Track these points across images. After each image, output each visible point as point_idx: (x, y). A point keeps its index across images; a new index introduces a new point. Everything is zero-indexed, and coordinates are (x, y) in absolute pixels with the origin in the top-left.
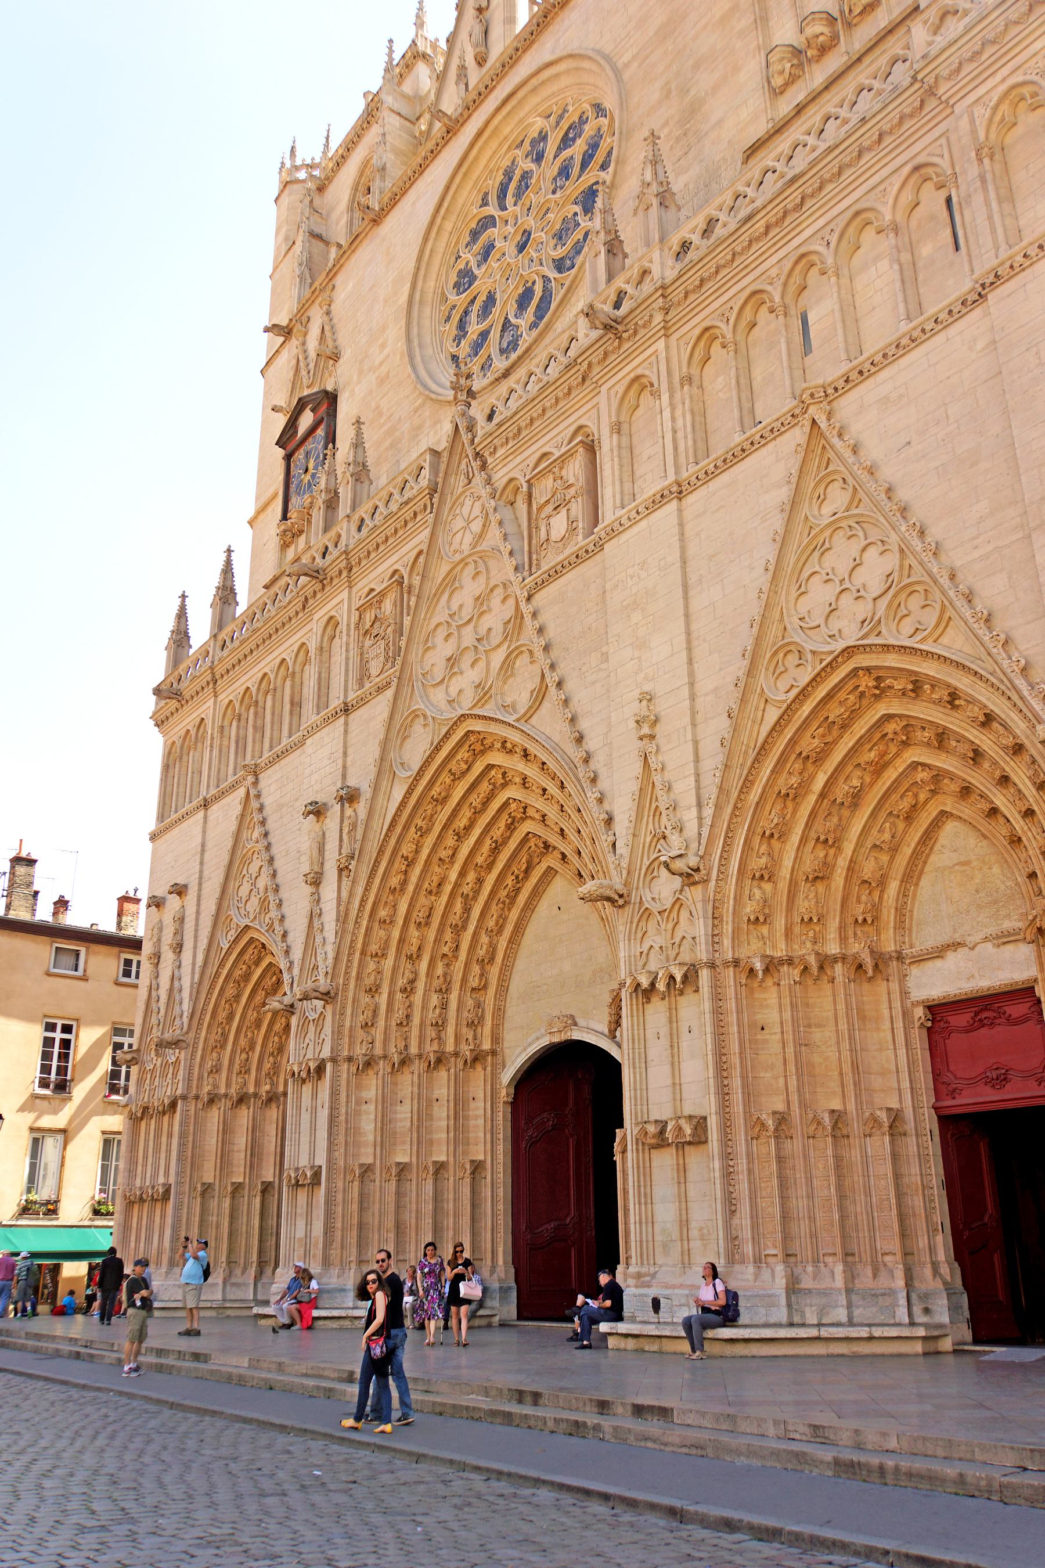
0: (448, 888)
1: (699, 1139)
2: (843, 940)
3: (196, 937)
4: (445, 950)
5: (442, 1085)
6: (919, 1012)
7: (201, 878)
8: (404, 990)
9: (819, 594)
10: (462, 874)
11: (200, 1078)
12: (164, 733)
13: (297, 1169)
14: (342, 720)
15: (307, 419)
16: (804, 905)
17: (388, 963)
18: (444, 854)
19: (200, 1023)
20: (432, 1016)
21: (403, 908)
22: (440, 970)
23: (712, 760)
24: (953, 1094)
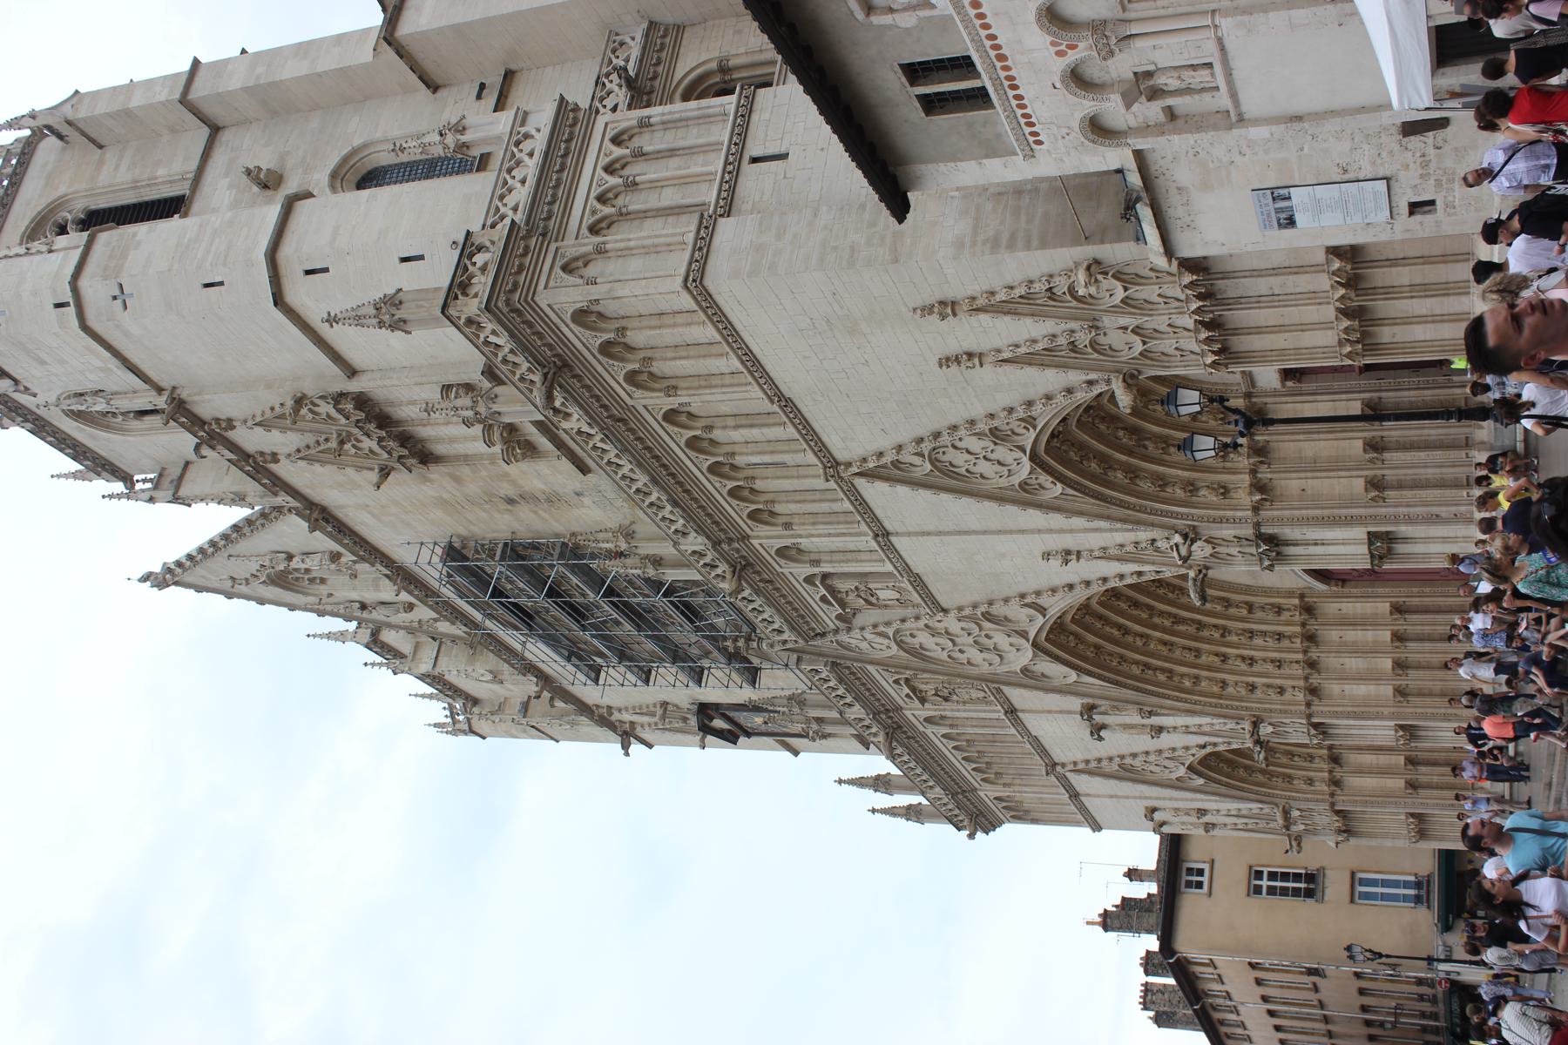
0: (1167, 637)
4: (1217, 635)
6: (1289, 384)
7: (1140, 798)
10: (1155, 627)
11: (1314, 792)
12: (1001, 823)
15: (719, 723)
18: (1139, 643)
19: (1269, 795)
20: (1271, 643)
22: (1234, 638)
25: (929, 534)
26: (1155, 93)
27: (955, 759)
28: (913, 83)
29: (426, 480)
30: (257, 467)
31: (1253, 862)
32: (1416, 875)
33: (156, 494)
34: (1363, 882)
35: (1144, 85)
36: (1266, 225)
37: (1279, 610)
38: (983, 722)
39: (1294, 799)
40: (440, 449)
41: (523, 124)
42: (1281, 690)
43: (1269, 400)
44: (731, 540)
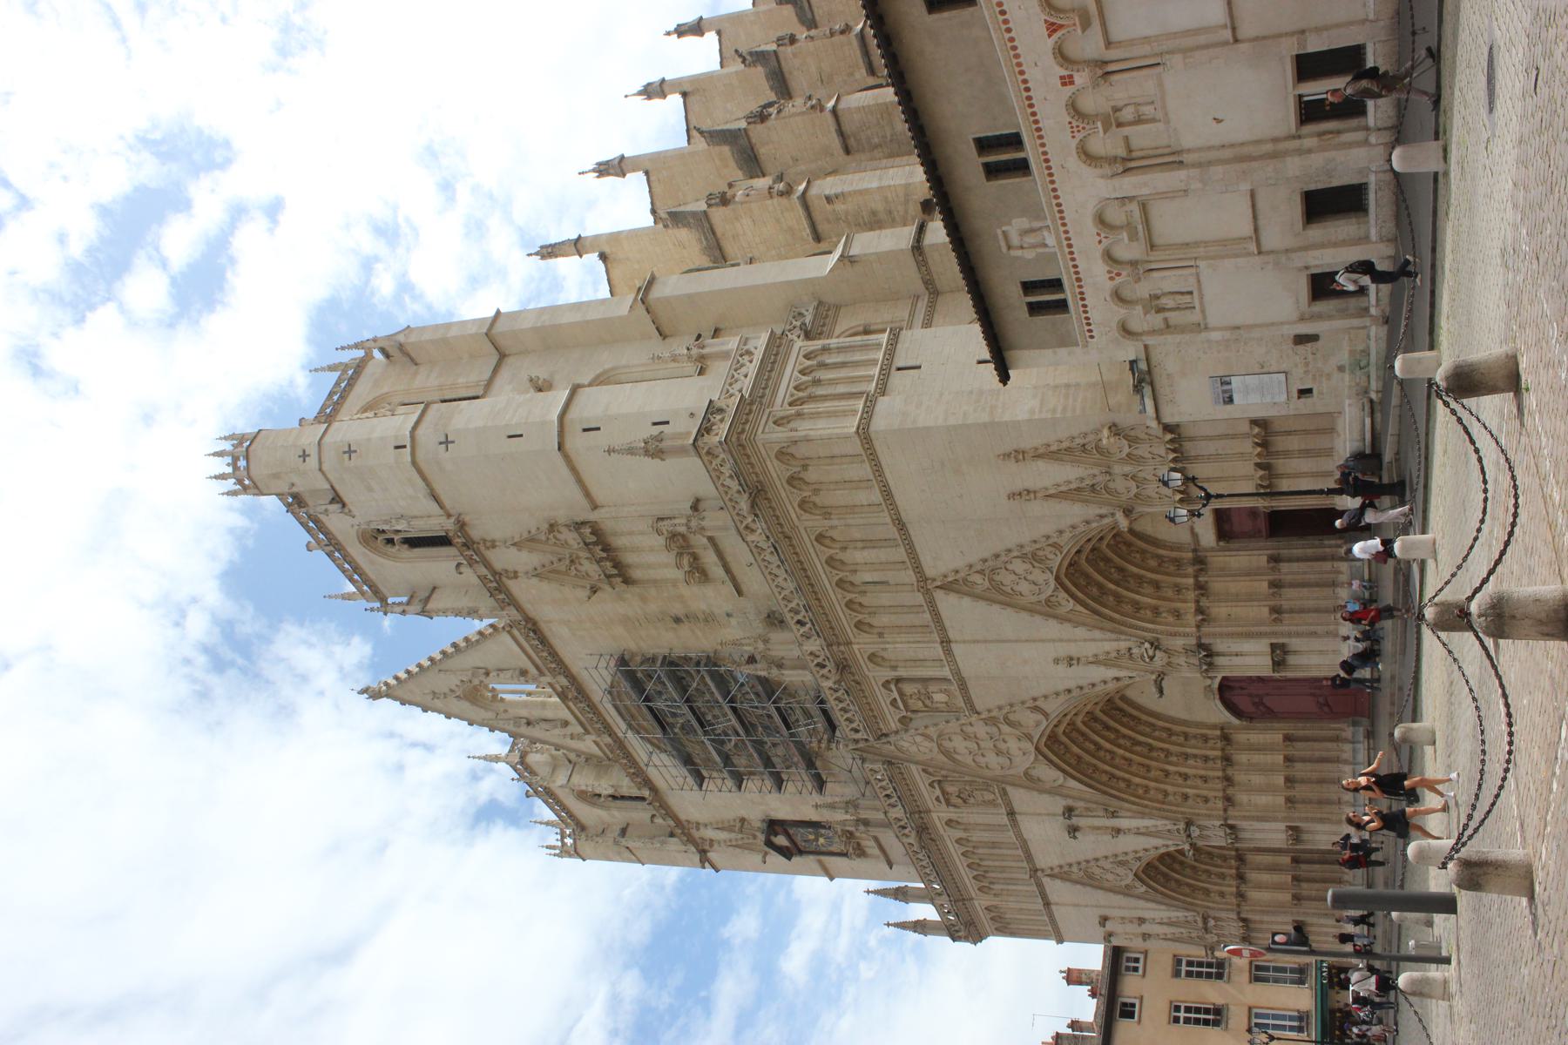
0: (1128, 755)
1: (1282, 647)
2: (1186, 576)
3: (1136, 908)
4: (1162, 756)
6: (1221, 544)
7: (1096, 906)
8: (1206, 781)
9: (1024, 587)
10: (1119, 746)
11: (1226, 903)
13: (1288, 840)
14: (1018, 817)
16: (1170, 593)
17: (1170, 788)
19: (1192, 904)
20: (1200, 763)
21: (1137, 780)
22: (1174, 759)
23: (1097, 634)
24: (1260, 531)
25: (978, 642)
26: (1160, 310)
27: (960, 864)
28: (1026, 294)
30: (498, 587)
31: (1173, 999)
32: (1298, 1011)
33: (406, 608)
34: (1258, 1016)
35: (1154, 304)
36: (1216, 402)
37: (1206, 739)
38: (989, 827)
39: (1213, 909)
40: (637, 574)
41: (745, 344)
42: (1206, 800)
43: (1208, 554)
44: (839, 644)
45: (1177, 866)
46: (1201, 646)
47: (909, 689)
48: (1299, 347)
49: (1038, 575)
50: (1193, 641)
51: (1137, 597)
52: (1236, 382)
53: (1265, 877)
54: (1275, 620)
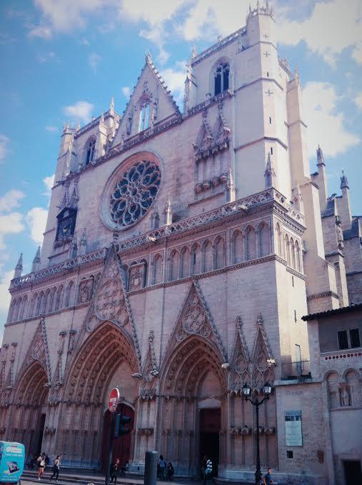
3: (19, 359)
5: (89, 412)
10: (101, 358)
14: (72, 311)
15: (67, 214)
16: (180, 385)
21: (84, 365)
26: (340, 391)
27: (50, 286)
29: (190, 158)
30: (201, 109)
35: (345, 387)
38: (68, 298)
40: (201, 165)
45: (36, 379)
46: (155, 397)
47: (142, 270)
48: (316, 454)
49: (195, 326)
50: (157, 393)
51: (179, 370)
52: (299, 423)
53: (26, 418)
54: (164, 432)
